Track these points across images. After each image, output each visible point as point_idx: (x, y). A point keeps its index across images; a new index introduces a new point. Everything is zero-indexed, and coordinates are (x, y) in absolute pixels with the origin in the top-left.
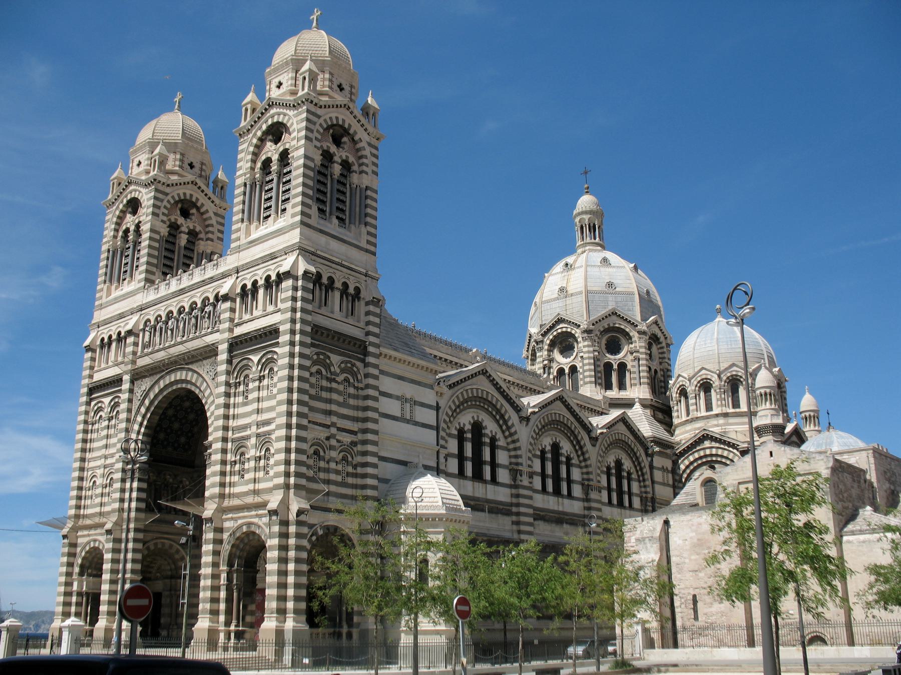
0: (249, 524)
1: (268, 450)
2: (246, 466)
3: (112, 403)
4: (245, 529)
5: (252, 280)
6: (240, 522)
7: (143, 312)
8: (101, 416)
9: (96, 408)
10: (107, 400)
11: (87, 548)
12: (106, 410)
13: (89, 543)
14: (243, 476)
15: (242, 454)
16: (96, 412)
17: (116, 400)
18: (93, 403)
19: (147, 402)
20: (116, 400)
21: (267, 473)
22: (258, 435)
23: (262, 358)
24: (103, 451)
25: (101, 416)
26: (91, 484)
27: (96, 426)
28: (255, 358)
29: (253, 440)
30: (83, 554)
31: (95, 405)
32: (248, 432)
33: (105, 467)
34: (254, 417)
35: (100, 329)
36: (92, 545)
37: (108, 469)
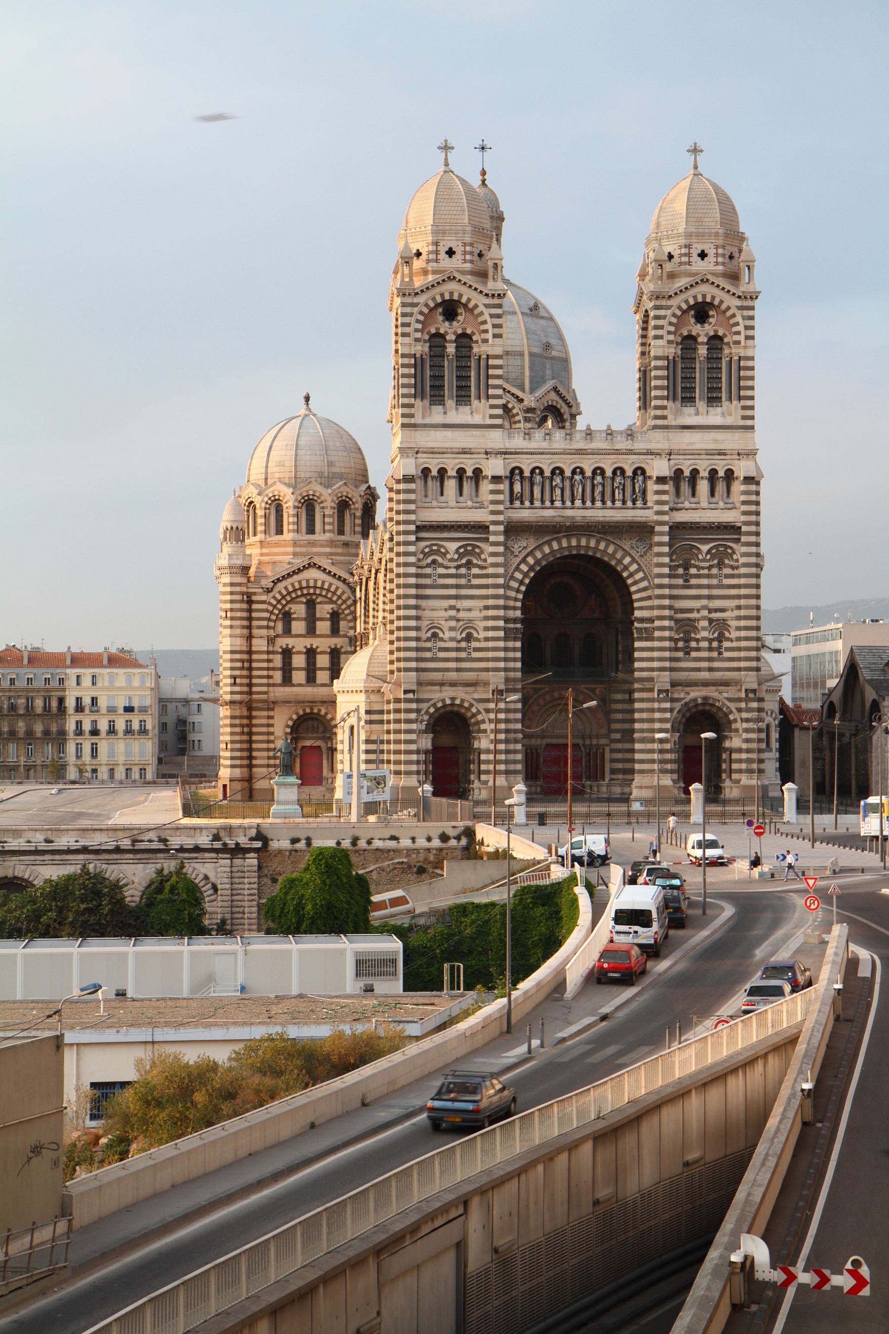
0: (705, 698)
1: (721, 635)
2: (693, 644)
3: (462, 550)
4: (700, 701)
5: (691, 468)
6: (693, 695)
7: (507, 456)
8: (434, 562)
9: (427, 550)
10: (452, 546)
11: (440, 705)
12: (448, 556)
13: (443, 701)
14: (687, 653)
15: (687, 633)
16: (426, 555)
17: (469, 548)
18: (423, 544)
19: (531, 560)
20: (469, 548)
21: (720, 653)
22: (711, 621)
23: (712, 548)
24: (452, 602)
25: (434, 562)
26: (429, 635)
27: (428, 571)
28: (705, 548)
29: (705, 623)
30: (432, 710)
31: (427, 547)
32: (694, 615)
33: (458, 620)
34: (704, 602)
35: (419, 455)
36: (448, 702)
37: (461, 623)
